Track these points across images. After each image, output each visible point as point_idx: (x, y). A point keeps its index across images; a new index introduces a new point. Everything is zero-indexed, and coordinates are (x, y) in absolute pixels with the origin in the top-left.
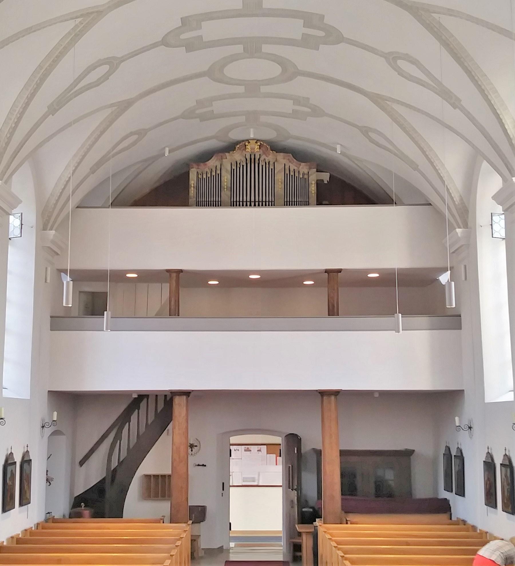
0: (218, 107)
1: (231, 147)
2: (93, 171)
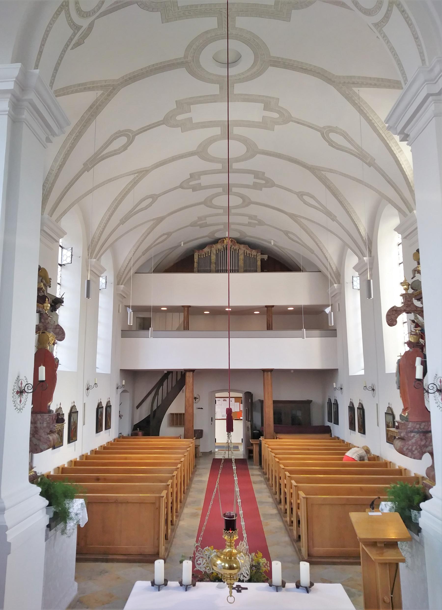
0: (209, 220)
1: (216, 241)
2: (144, 254)
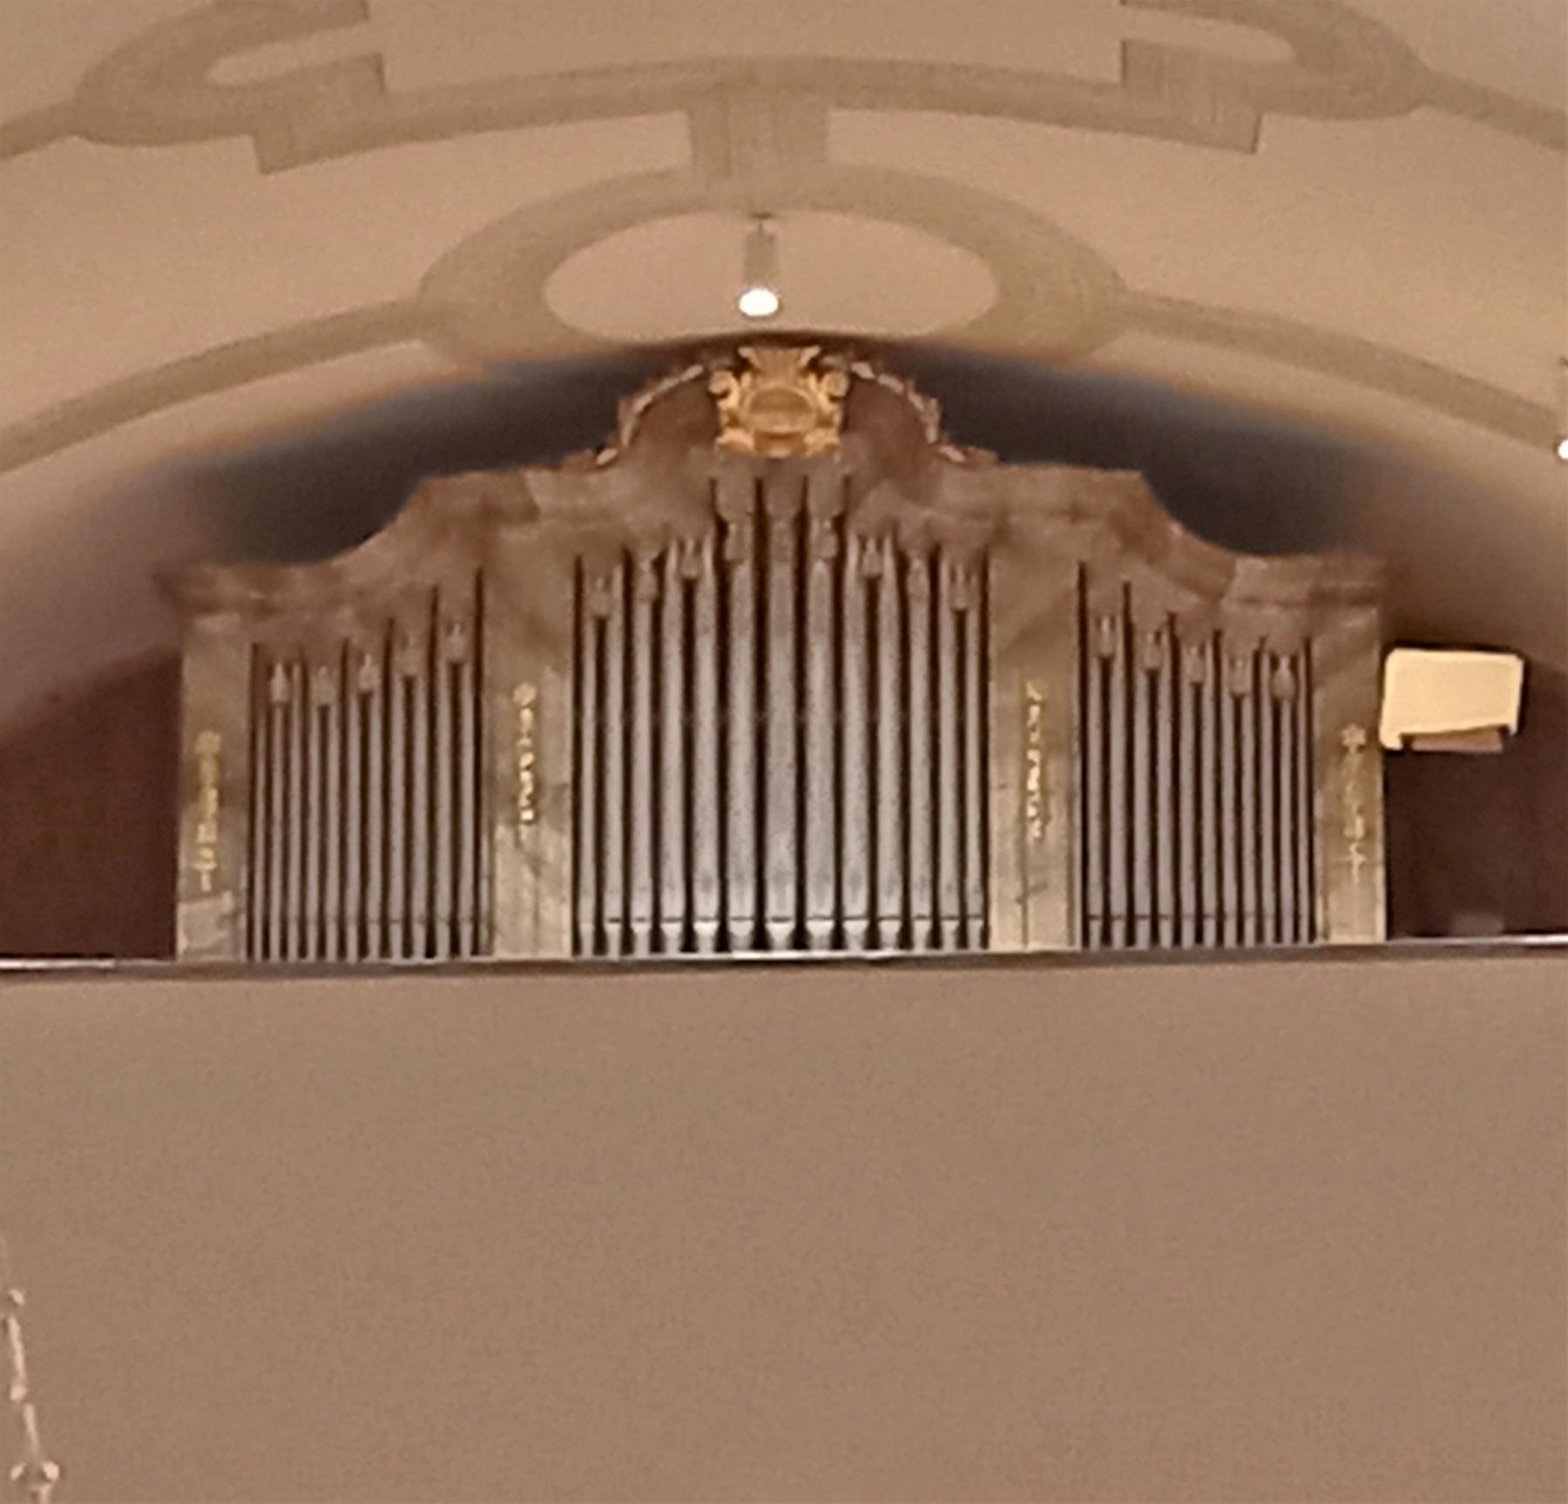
1: (567, 409)
